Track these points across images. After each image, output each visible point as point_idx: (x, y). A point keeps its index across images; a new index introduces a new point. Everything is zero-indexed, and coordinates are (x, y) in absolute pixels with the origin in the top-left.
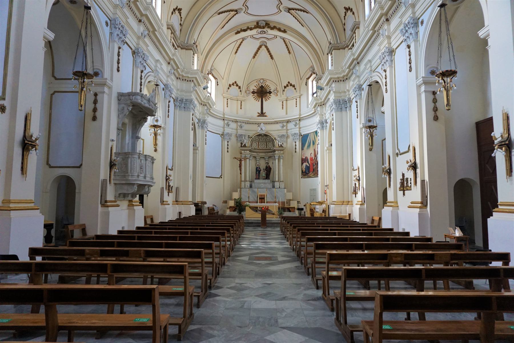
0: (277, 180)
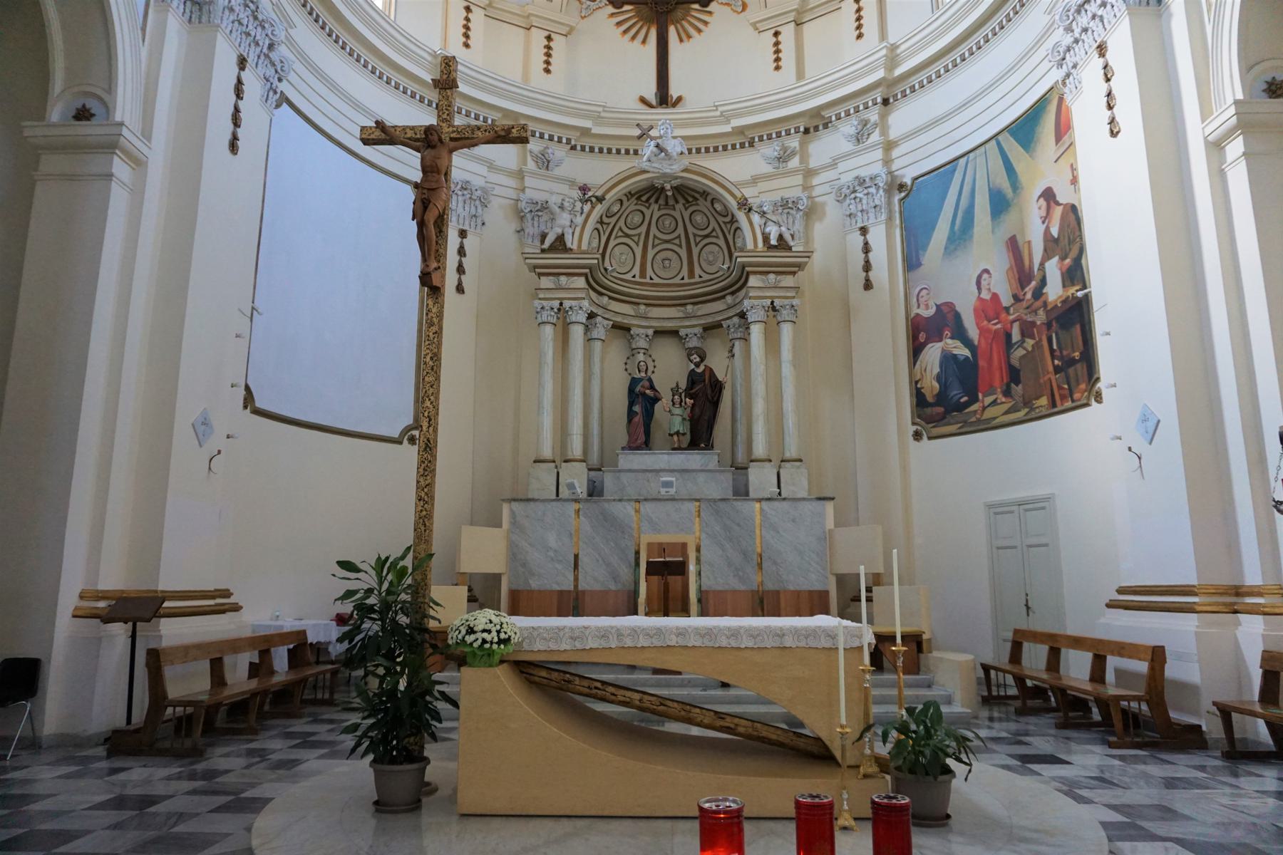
0: (760, 449)
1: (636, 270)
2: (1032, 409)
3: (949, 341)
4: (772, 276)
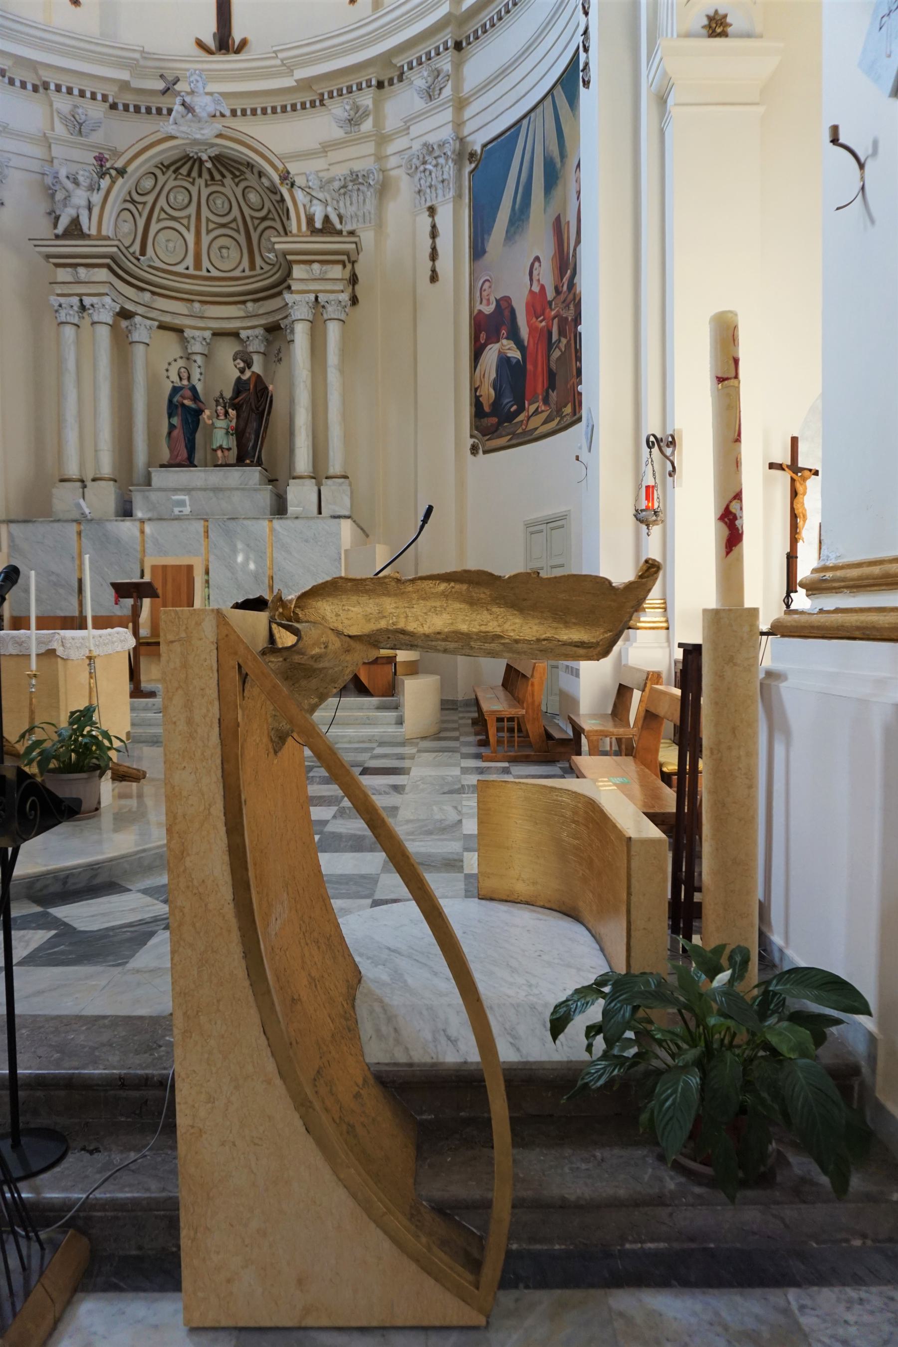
1: (190, 261)
2: (562, 418)
3: (505, 342)
4: (316, 266)
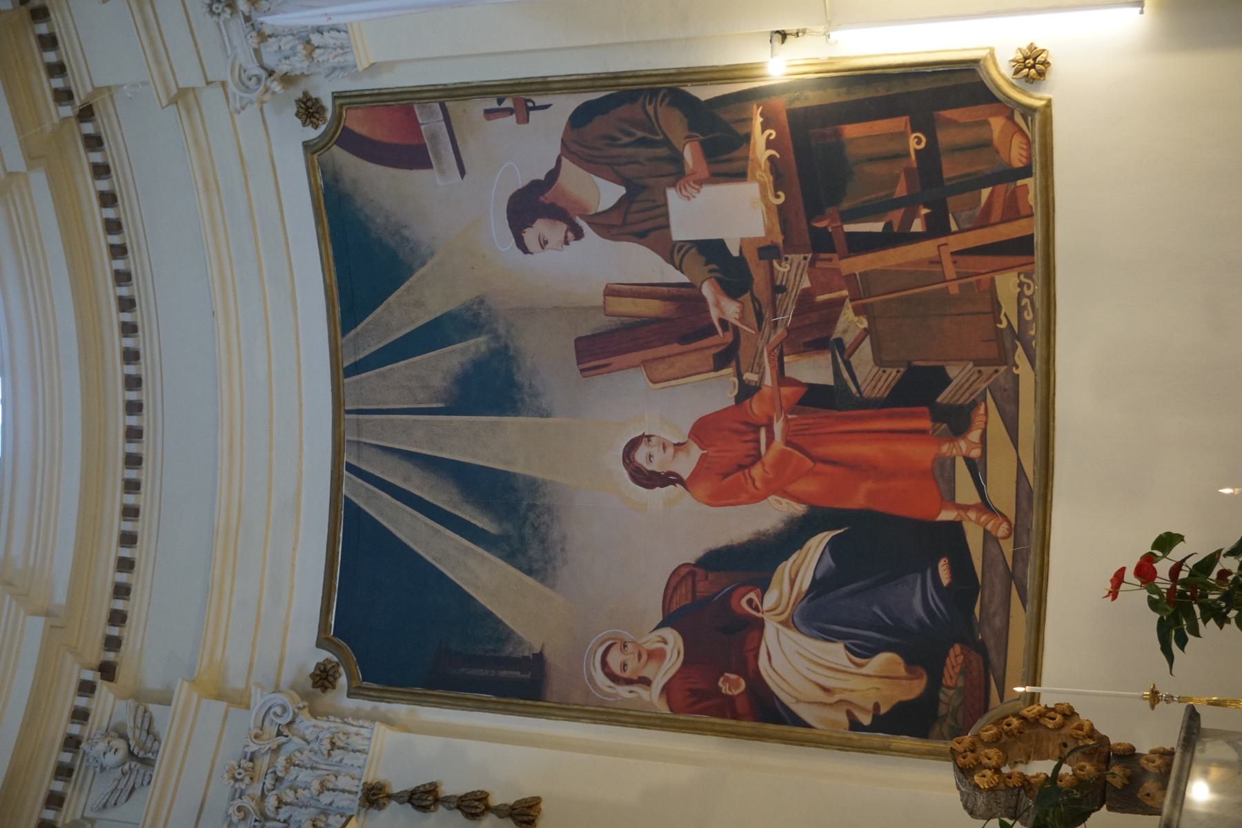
2: (1019, 335)
3: (770, 598)
